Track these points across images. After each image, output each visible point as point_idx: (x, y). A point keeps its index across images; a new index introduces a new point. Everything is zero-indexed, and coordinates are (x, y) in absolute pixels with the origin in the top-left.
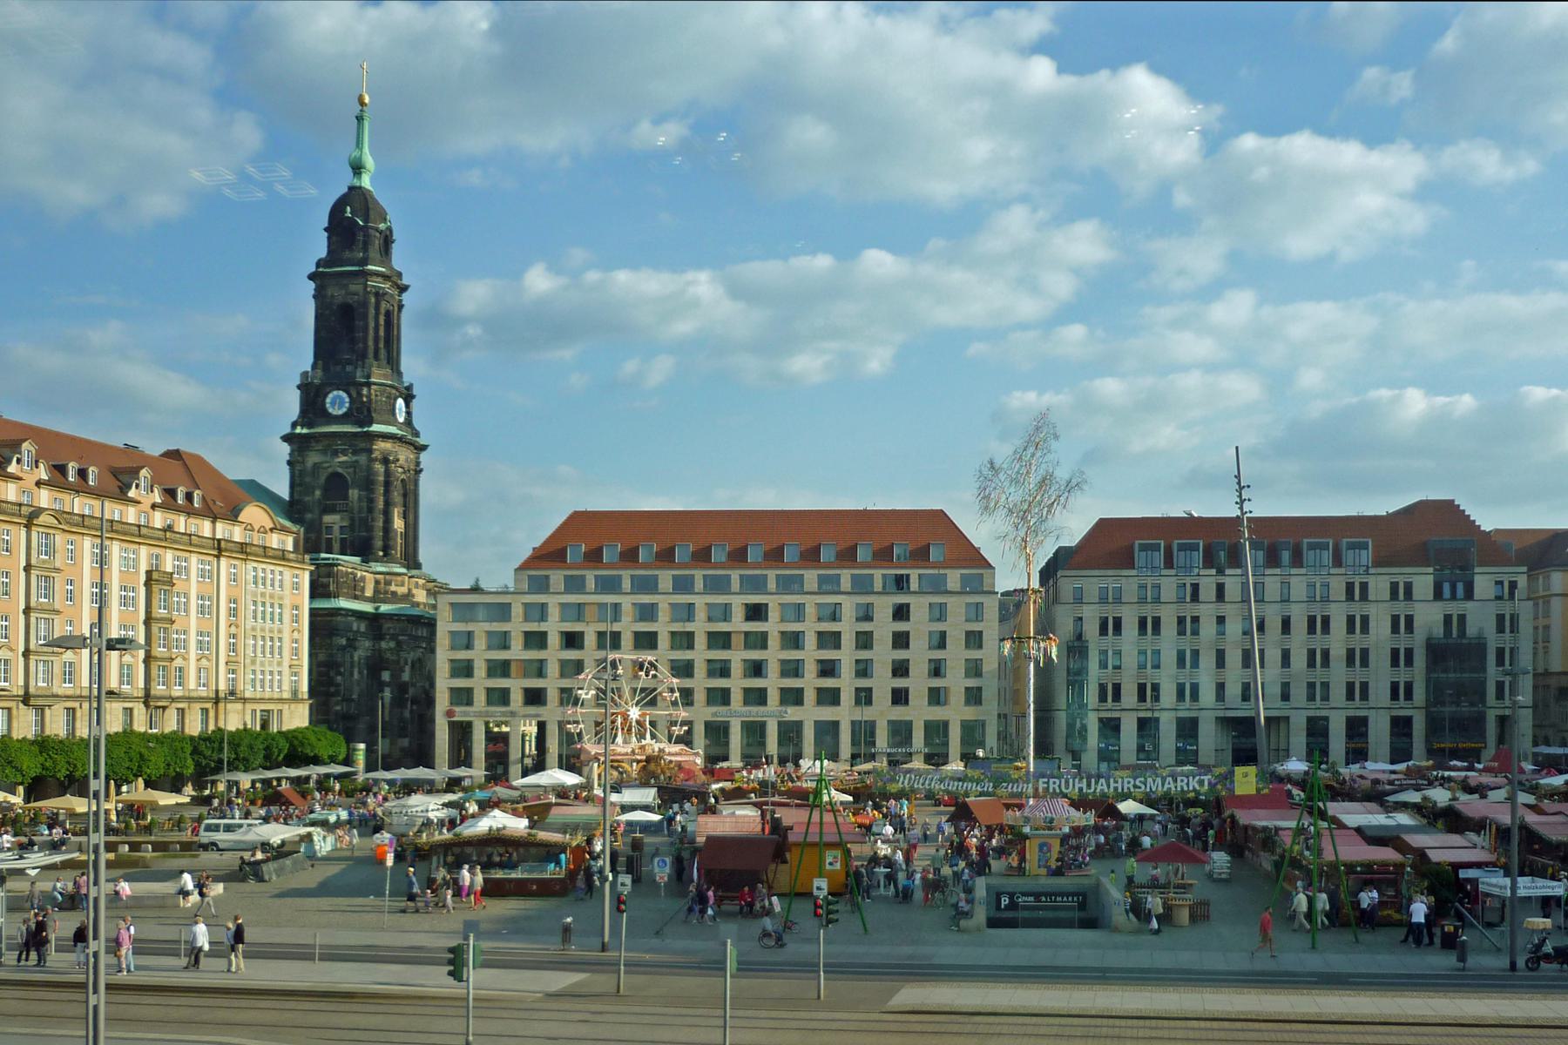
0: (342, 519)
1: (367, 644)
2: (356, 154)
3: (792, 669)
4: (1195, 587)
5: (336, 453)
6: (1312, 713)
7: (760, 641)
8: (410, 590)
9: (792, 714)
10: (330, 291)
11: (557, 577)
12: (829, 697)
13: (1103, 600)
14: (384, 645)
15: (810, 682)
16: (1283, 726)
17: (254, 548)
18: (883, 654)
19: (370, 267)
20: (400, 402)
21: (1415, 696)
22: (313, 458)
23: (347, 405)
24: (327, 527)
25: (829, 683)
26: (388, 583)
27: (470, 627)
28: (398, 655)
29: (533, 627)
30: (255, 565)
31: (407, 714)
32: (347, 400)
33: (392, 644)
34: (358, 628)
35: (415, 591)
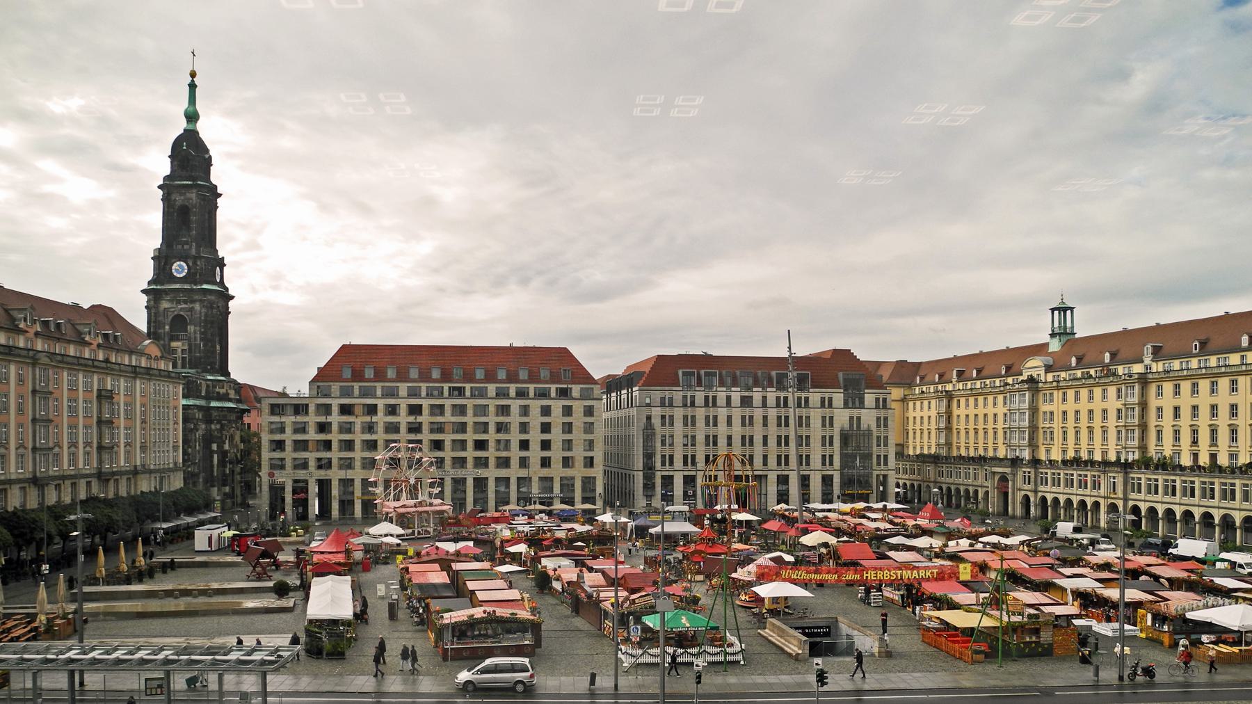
0: (183, 345)
1: (203, 426)
4: (714, 398)
5: (179, 302)
6: (779, 473)
7: (462, 428)
9: (482, 473)
10: (174, 197)
11: (335, 387)
12: (504, 463)
13: (663, 404)
14: (213, 427)
16: (763, 480)
18: (535, 437)
19: (199, 182)
20: (218, 268)
22: (165, 305)
23: (186, 271)
26: (214, 387)
28: (221, 433)
29: (322, 419)
32: (186, 267)
35: (229, 391)
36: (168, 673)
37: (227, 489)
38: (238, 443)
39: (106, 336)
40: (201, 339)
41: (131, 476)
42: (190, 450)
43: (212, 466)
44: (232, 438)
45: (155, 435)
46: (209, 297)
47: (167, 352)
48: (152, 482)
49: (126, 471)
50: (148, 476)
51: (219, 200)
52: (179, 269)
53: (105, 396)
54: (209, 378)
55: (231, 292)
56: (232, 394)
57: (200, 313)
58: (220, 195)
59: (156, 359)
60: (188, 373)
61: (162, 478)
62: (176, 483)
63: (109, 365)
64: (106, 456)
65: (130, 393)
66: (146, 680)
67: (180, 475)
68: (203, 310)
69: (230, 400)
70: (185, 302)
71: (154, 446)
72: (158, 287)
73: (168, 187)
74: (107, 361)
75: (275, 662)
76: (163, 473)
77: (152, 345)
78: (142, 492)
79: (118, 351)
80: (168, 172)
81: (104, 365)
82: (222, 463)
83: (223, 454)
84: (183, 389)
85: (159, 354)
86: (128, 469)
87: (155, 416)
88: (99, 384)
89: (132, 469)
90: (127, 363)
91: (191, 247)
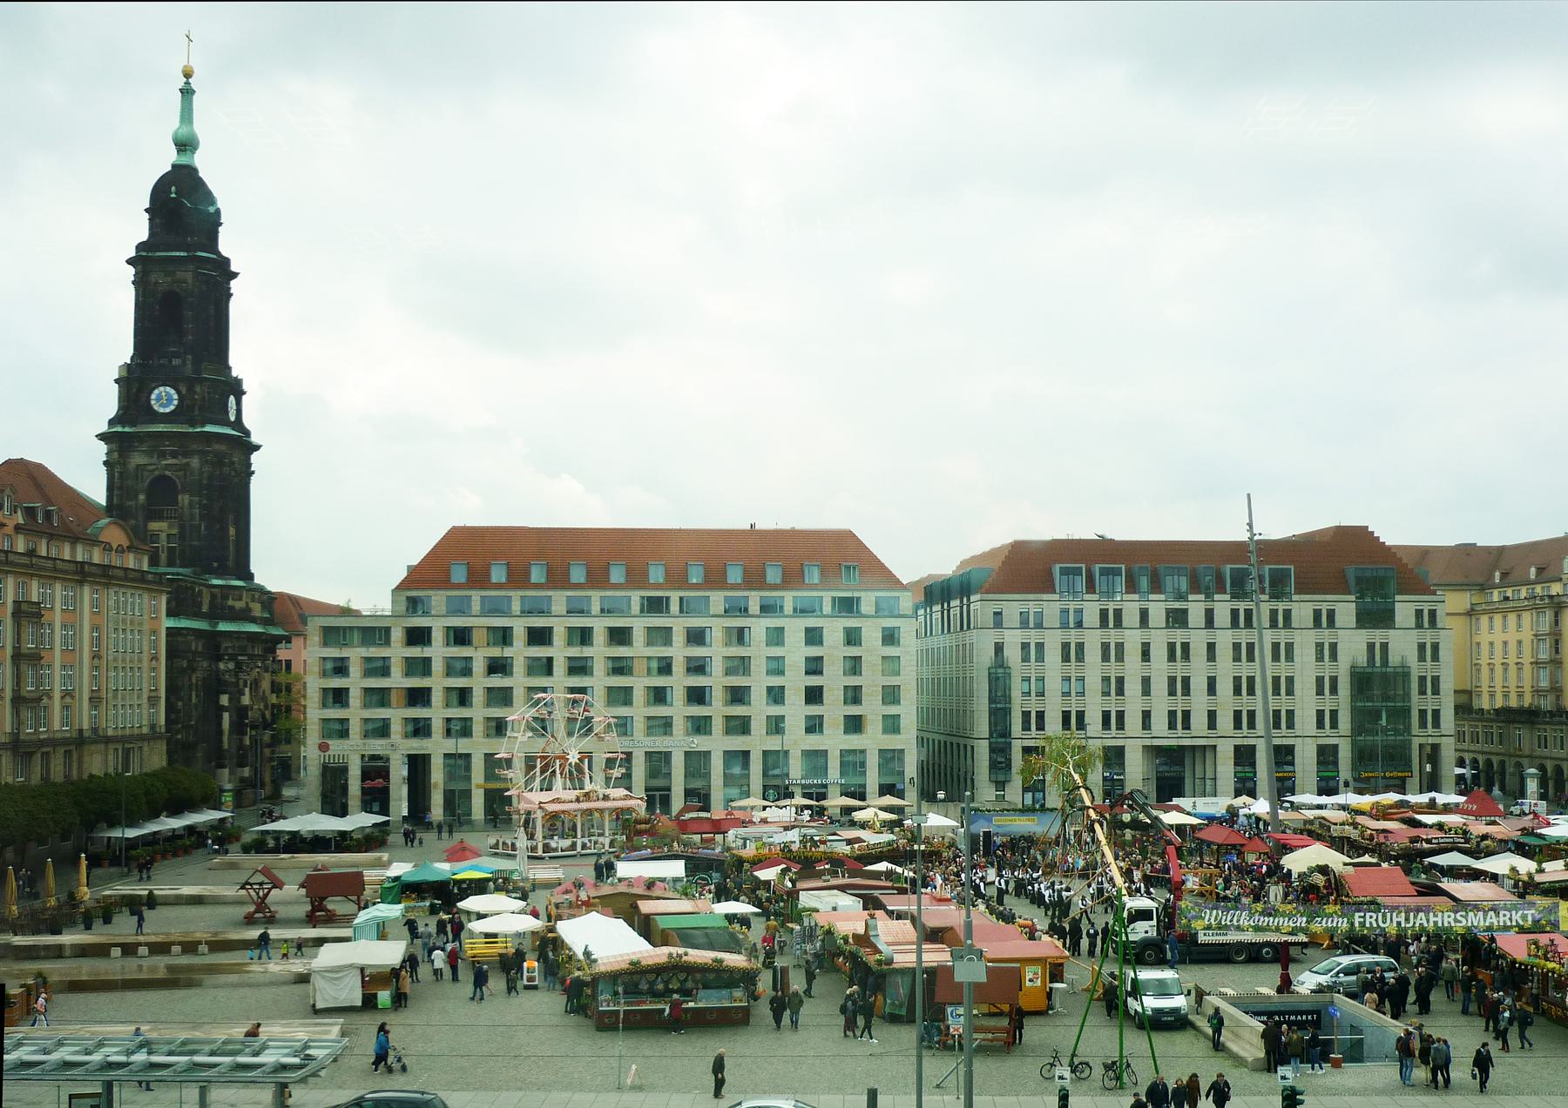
0: (170, 527)
2: (184, 131)
3: (697, 696)
5: (163, 455)
8: (247, 603)
10: (153, 278)
14: (222, 666)
15: (718, 709)
17: (115, 571)
20: (232, 398)
21: (1340, 725)
22: (137, 459)
23: (176, 402)
24: (151, 535)
25: (738, 710)
27: (344, 653)
28: (236, 676)
30: (116, 589)
31: (247, 741)
32: (176, 397)
33: (231, 666)
34: (196, 648)
35: (252, 605)
36: (109, 1086)
37: (246, 772)
38: (268, 692)
39: (30, 512)
40: (202, 517)
41: (72, 747)
42: (180, 704)
43: (220, 732)
44: (255, 685)
45: (116, 677)
46: (217, 447)
47: (140, 539)
48: (111, 757)
49: (64, 738)
50: (102, 747)
51: (233, 283)
52: (164, 398)
53: (27, 614)
54: (216, 582)
55: (254, 439)
56: (257, 609)
57: (201, 473)
58: (235, 275)
59: (121, 550)
60: (178, 574)
61: (127, 752)
62: (155, 758)
63: (34, 560)
64: (27, 714)
65: (71, 610)
66: (71, 1097)
67: (162, 747)
68: (206, 469)
69: (254, 620)
70: (174, 455)
71: (115, 697)
72: (127, 429)
73: (143, 260)
74: (31, 553)
75: (301, 1067)
76: (127, 743)
77: (112, 526)
78: (91, 776)
79: (51, 537)
80: (143, 234)
81: (25, 560)
82: (239, 727)
83: (240, 712)
84: (168, 603)
85: (126, 543)
86: (68, 735)
87: (116, 646)
88: (16, 593)
89: (75, 735)
90: (67, 557)
91: (184, 362)
